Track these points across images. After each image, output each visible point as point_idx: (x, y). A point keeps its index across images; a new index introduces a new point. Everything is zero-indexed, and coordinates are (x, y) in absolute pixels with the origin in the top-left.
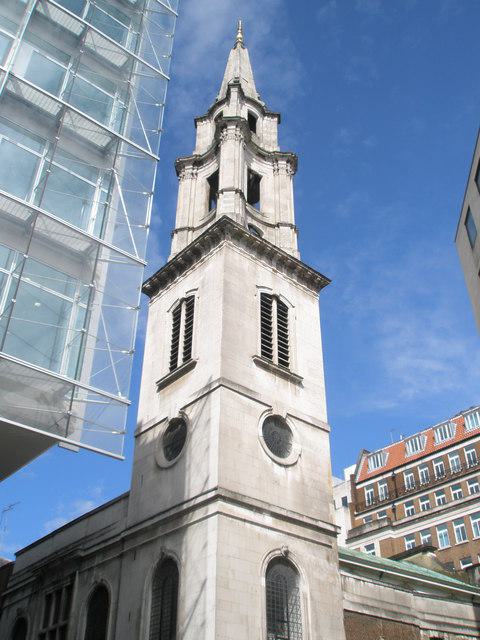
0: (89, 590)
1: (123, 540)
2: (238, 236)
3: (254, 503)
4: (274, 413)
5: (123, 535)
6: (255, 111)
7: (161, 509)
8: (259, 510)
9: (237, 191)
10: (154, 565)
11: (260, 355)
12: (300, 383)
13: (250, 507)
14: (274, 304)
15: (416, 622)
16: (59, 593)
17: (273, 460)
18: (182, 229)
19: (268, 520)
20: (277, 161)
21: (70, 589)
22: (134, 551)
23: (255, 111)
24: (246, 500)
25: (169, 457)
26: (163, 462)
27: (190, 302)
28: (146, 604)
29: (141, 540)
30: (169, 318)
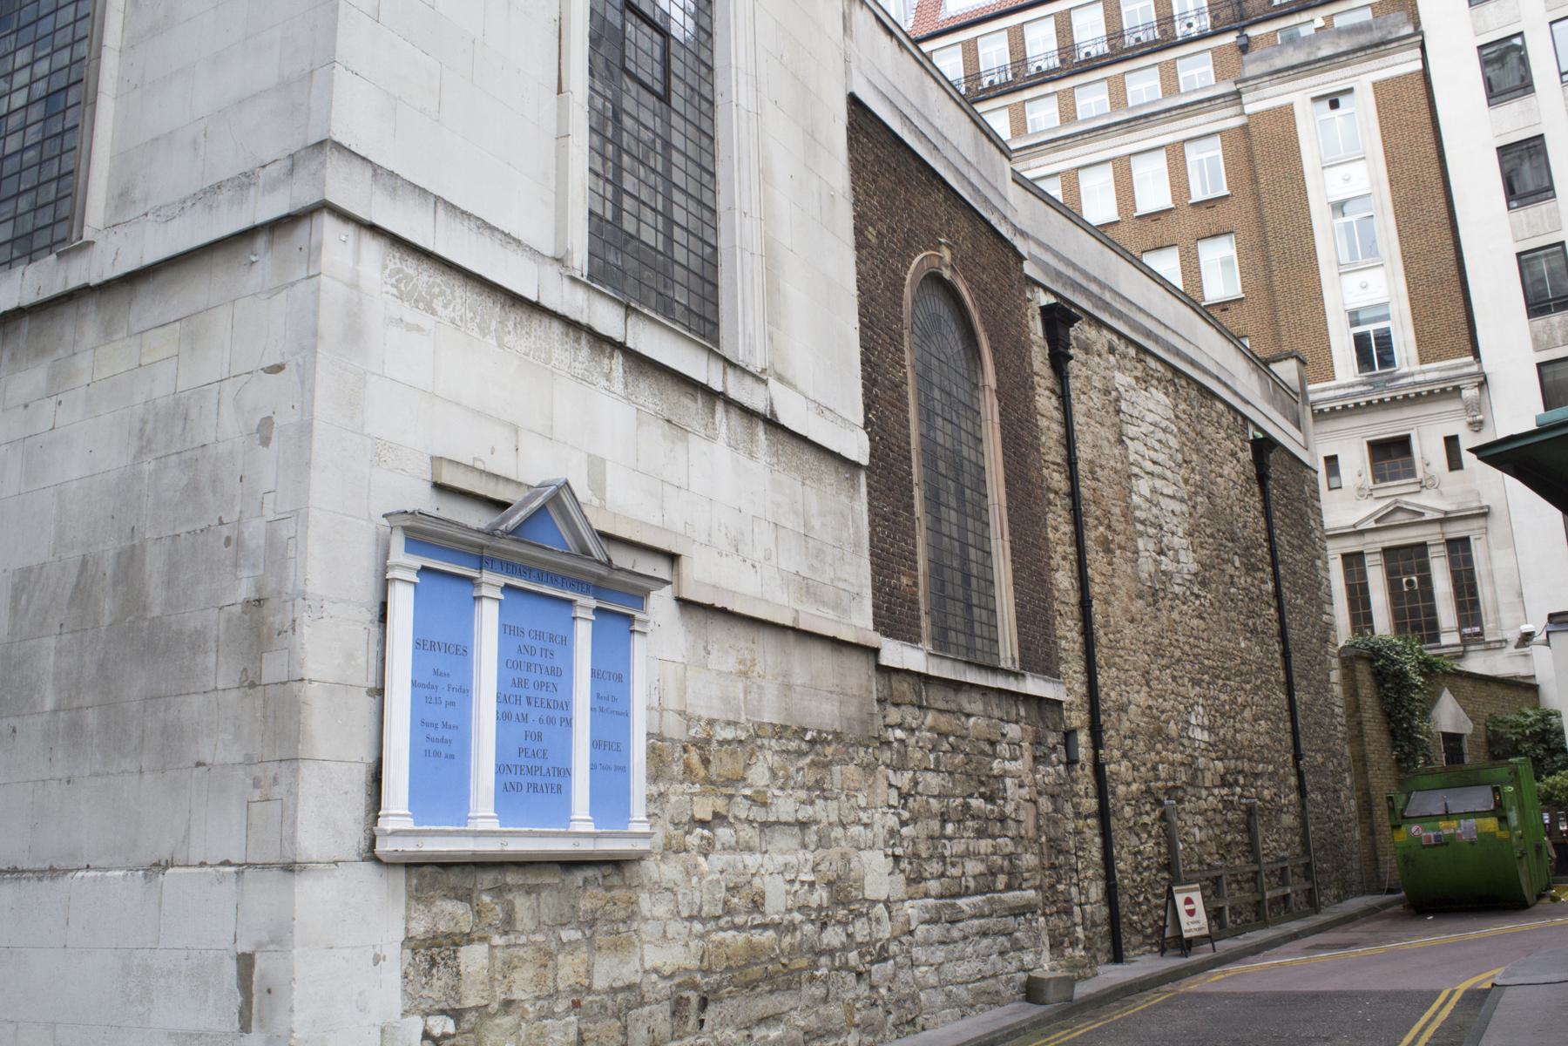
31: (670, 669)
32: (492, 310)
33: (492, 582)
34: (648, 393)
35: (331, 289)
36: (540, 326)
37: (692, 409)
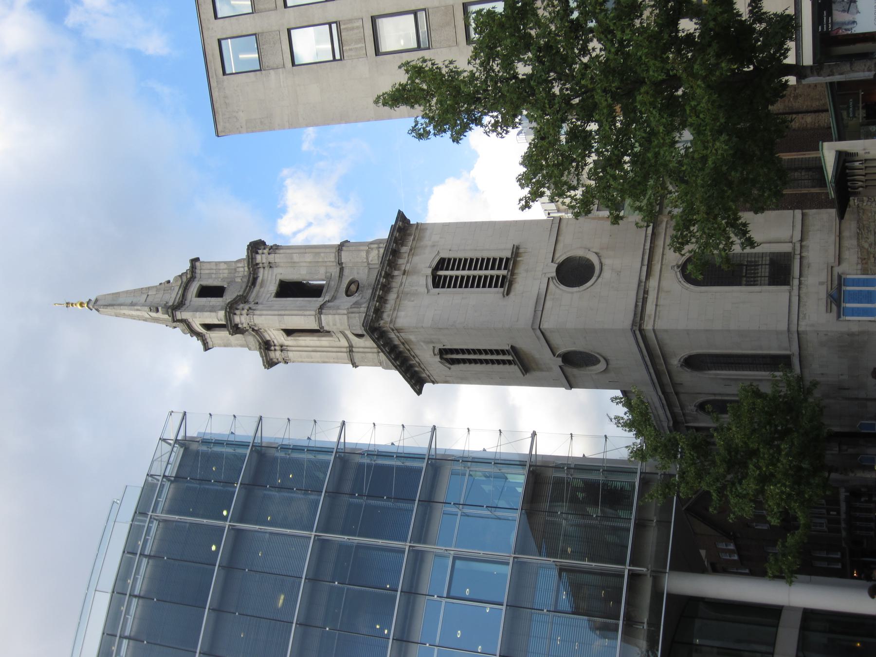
0: (702, 416)
1: (664, 392)
2: (379, 312)
3: (641, 296)
4: (554, 274)
5: (660, 393)
6: (194, 288)
7: (643, 367)
8: (646, 292)
9: (320, 313)
10: (689, 370)
11: (502, 289)
12: (518, 248)
13: (645, 300)
17: (599, 276)
19: (653, 283)
20: (257, 264)
21: (698, 429)
22: (674, 385)
23: (194, 288)
24: (640, 304)
25: (597, 361)
26: (602, 366)
28: (718, 375)
29: (666, 379)
30: (462, 366)
31: (851, 268)
32: (801, 304)
33: (843, 305)
34: (805, 272)
35: (808, 329)
36: (802, 295)
37: (805, 262)
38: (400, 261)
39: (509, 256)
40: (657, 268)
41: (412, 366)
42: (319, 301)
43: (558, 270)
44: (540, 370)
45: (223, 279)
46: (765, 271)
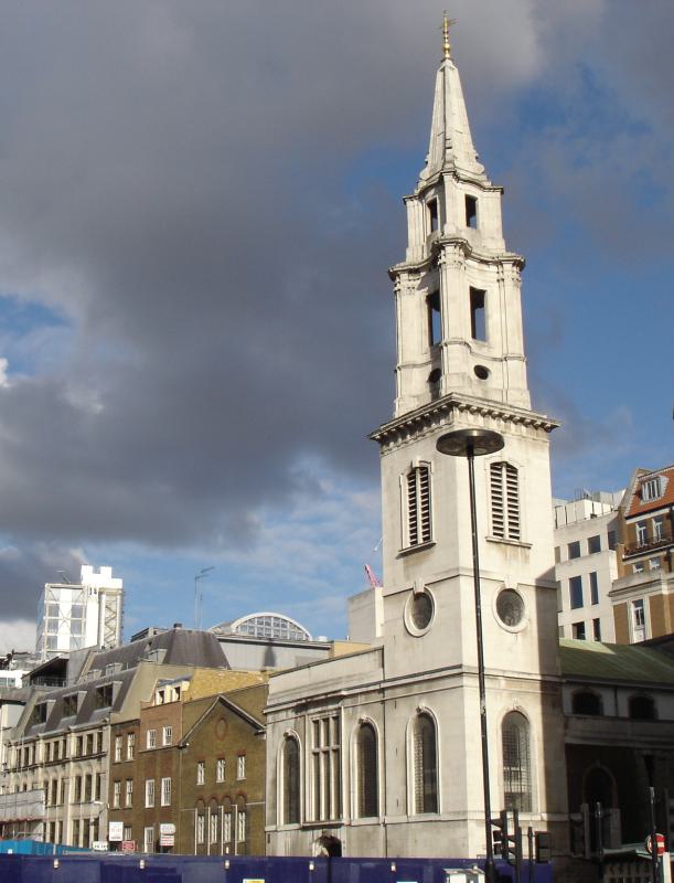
4: (508, 587)
6: (473, 191)
11: (491, 534)
14: (504, 470)
15: (631, 745)
16: (326, 720)
18: (404, 366)
19: (503, 682)
20: (502, 265)
21: (337, 719)
23: (473, 191)
27: (424, 471)
30: (406, 487)
38: (513, 425)
39: (524, 540)
40: (516, 687)
41: (404, 437)
42: (469, 339)
43: (512, 591)
44: (406, 568)
45: (483, 224)
46: (515, 789)
